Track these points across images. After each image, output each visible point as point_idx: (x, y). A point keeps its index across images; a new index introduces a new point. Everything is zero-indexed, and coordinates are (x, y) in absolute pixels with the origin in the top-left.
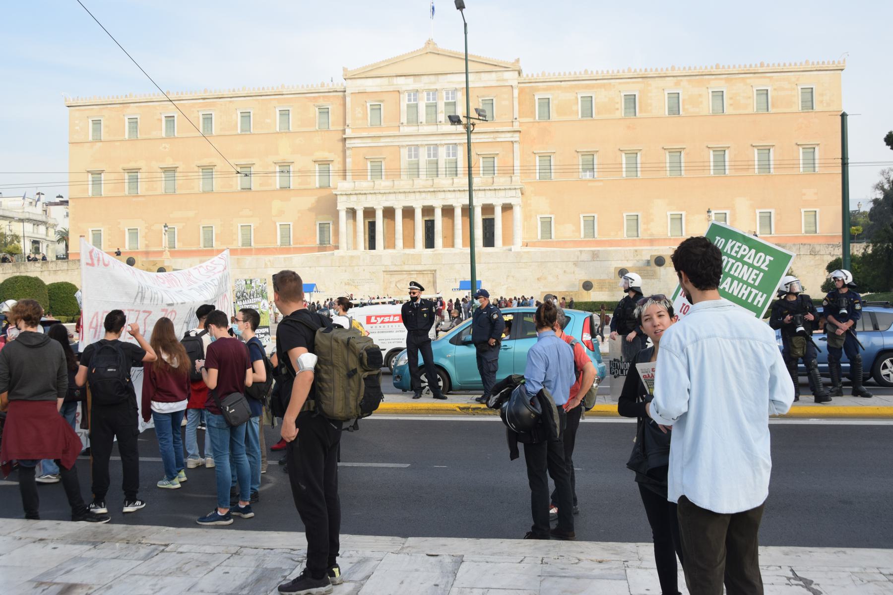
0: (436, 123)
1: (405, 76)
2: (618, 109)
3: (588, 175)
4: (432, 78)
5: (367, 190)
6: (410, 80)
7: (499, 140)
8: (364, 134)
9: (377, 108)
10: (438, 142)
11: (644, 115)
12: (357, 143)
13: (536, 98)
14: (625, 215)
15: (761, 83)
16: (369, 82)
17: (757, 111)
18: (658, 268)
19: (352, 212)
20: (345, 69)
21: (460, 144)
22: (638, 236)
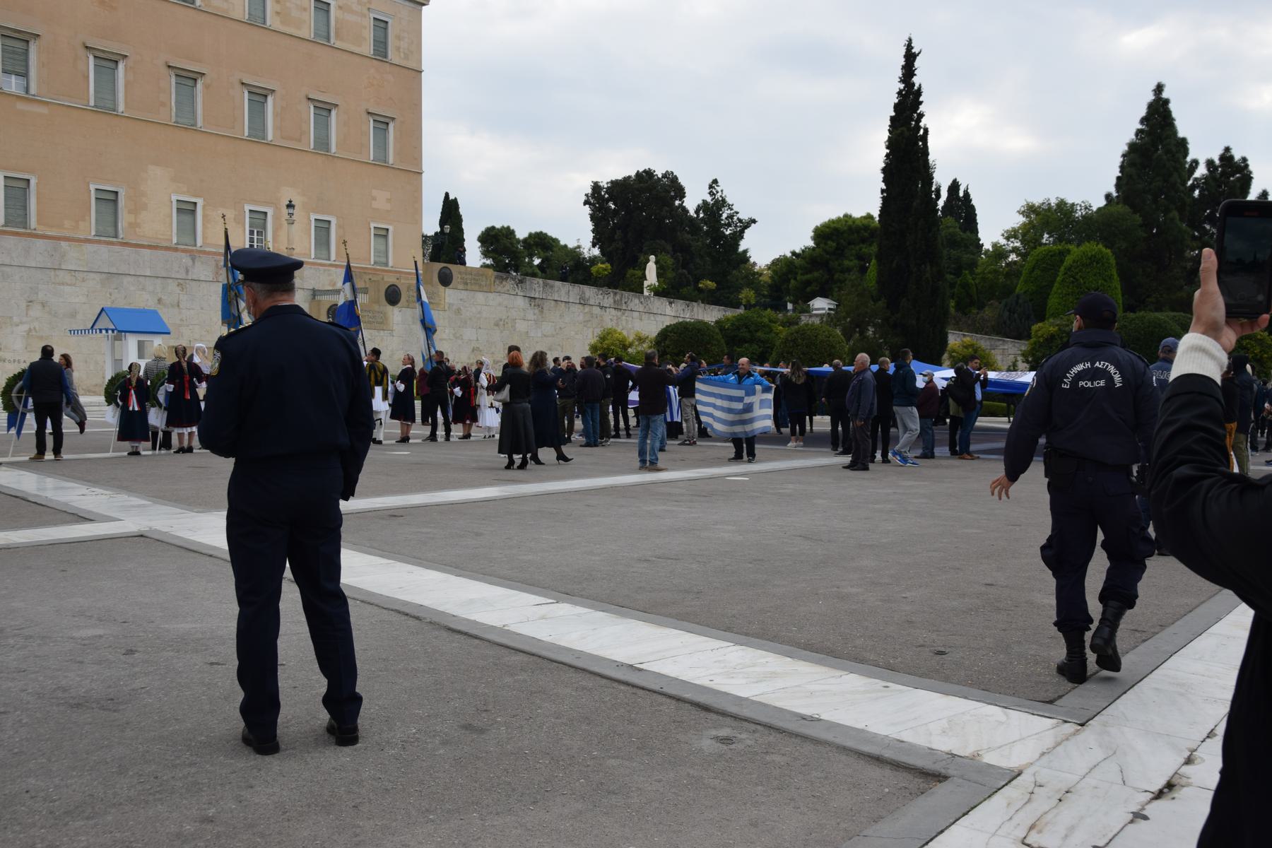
3: (13, 84)
14: (92, 187)
17: (314, 38)
18: (389, 308)
22: (116, 237)
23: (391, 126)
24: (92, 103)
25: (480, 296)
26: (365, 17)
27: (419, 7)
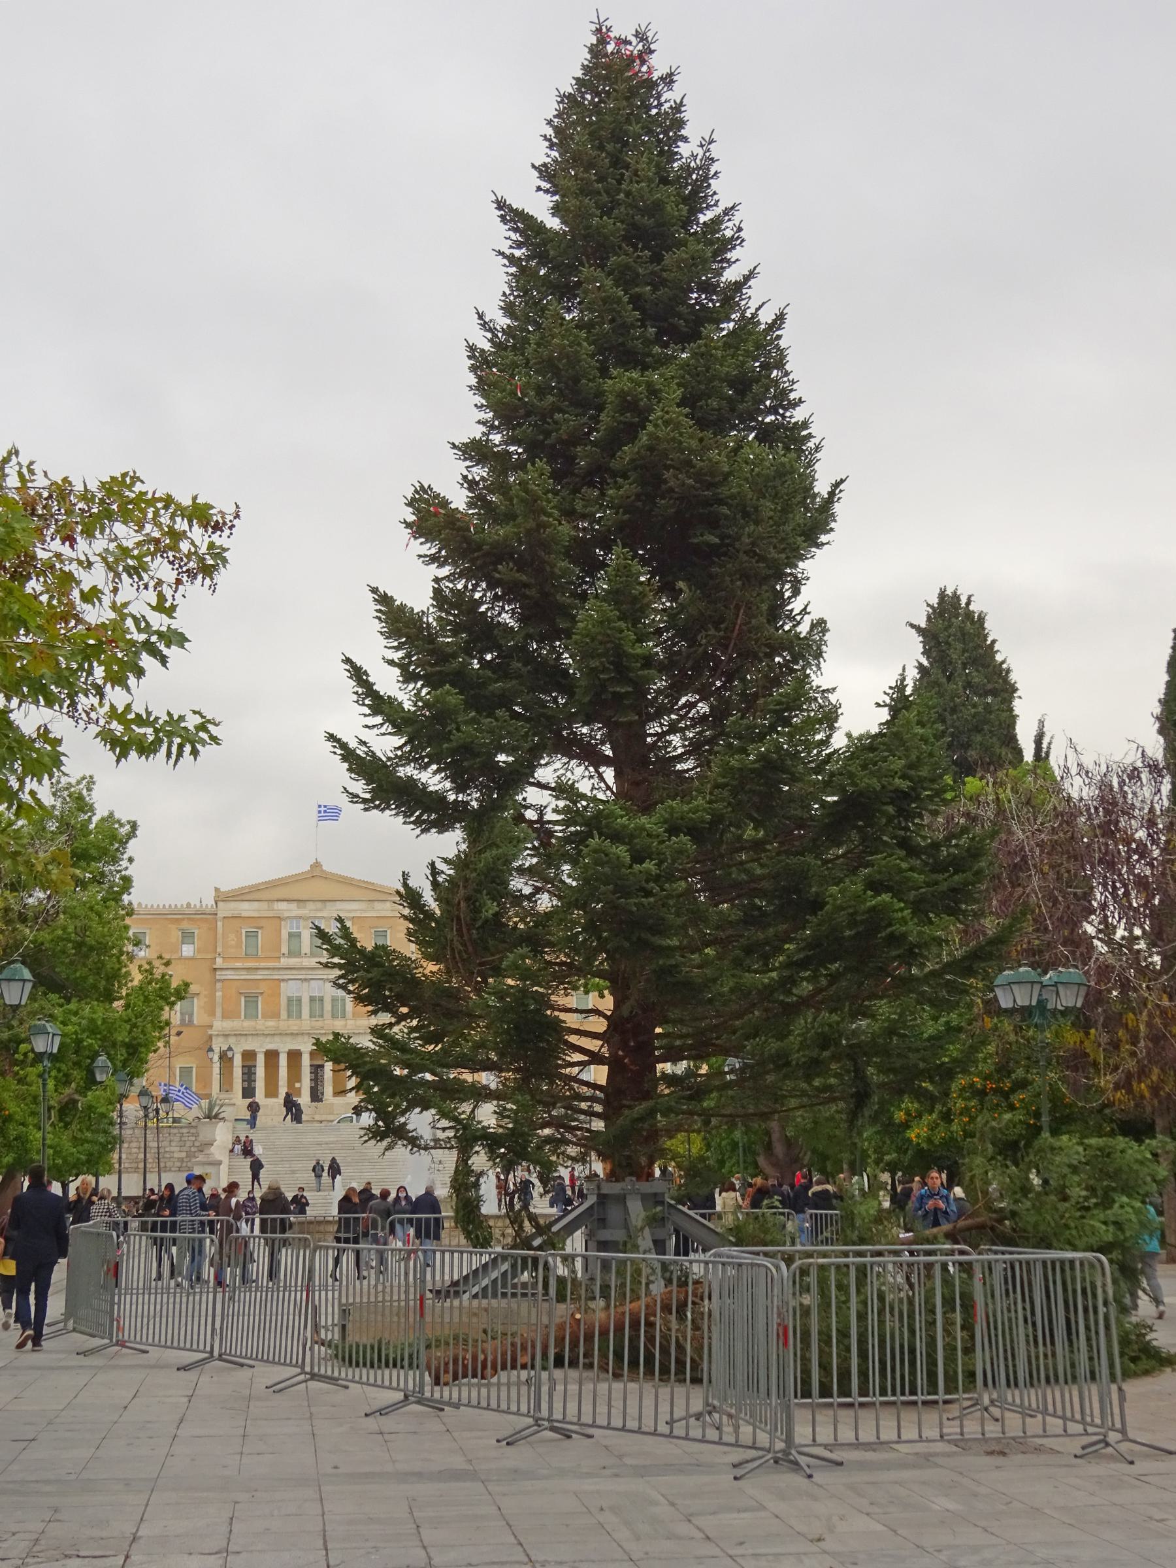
4: (319, 905)
6: (293, 906)
8: (238, 965)
9: (252, 935)
12: (230, 975)
16: (245, 905)
20: (217, 890)
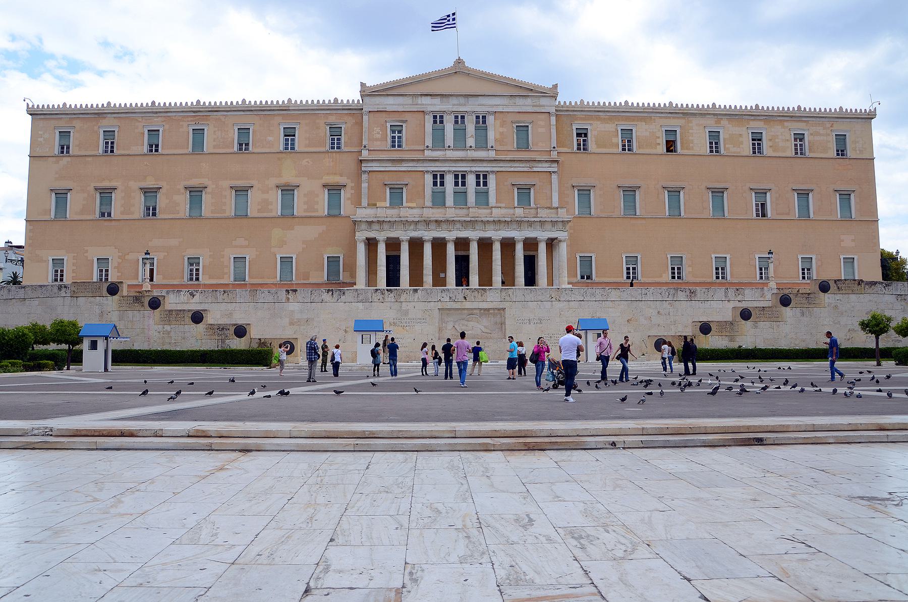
0: (464, 148)
1: (431, 95)
2: (659, 144)
4: (462, 100)
5: (392, 217)
6: (437, 101)
7: (535, 169)
9: (397, 129)
10: (468, 169)
11: (686, 152)
12: (375, 167)
13: (574, 128)
15: (798, 127)
19: (371, 244)
20: (363, 85)
21: (492, 172)
23: (852, 196)
24: (667, 214)
25: (853, 297)
26: (829, 135)
27: (869, 120)
